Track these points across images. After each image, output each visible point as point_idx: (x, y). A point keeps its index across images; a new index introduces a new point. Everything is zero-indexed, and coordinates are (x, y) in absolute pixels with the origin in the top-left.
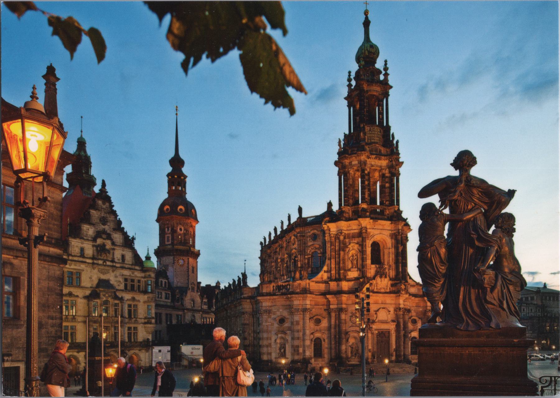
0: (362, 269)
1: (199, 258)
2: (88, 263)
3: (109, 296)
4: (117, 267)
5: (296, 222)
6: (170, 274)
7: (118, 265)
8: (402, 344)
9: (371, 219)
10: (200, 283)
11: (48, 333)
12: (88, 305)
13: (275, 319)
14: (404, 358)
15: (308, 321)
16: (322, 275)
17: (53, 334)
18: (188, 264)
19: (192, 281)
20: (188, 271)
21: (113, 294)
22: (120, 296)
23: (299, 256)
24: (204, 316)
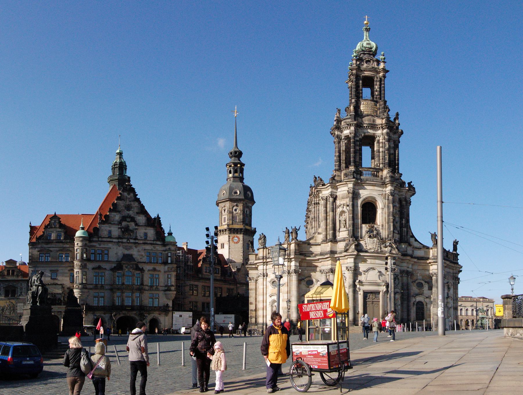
1: (255, 235)
3: (131, 268)
4: (139, 244)
7: (139, 242)
21: (135, 266)
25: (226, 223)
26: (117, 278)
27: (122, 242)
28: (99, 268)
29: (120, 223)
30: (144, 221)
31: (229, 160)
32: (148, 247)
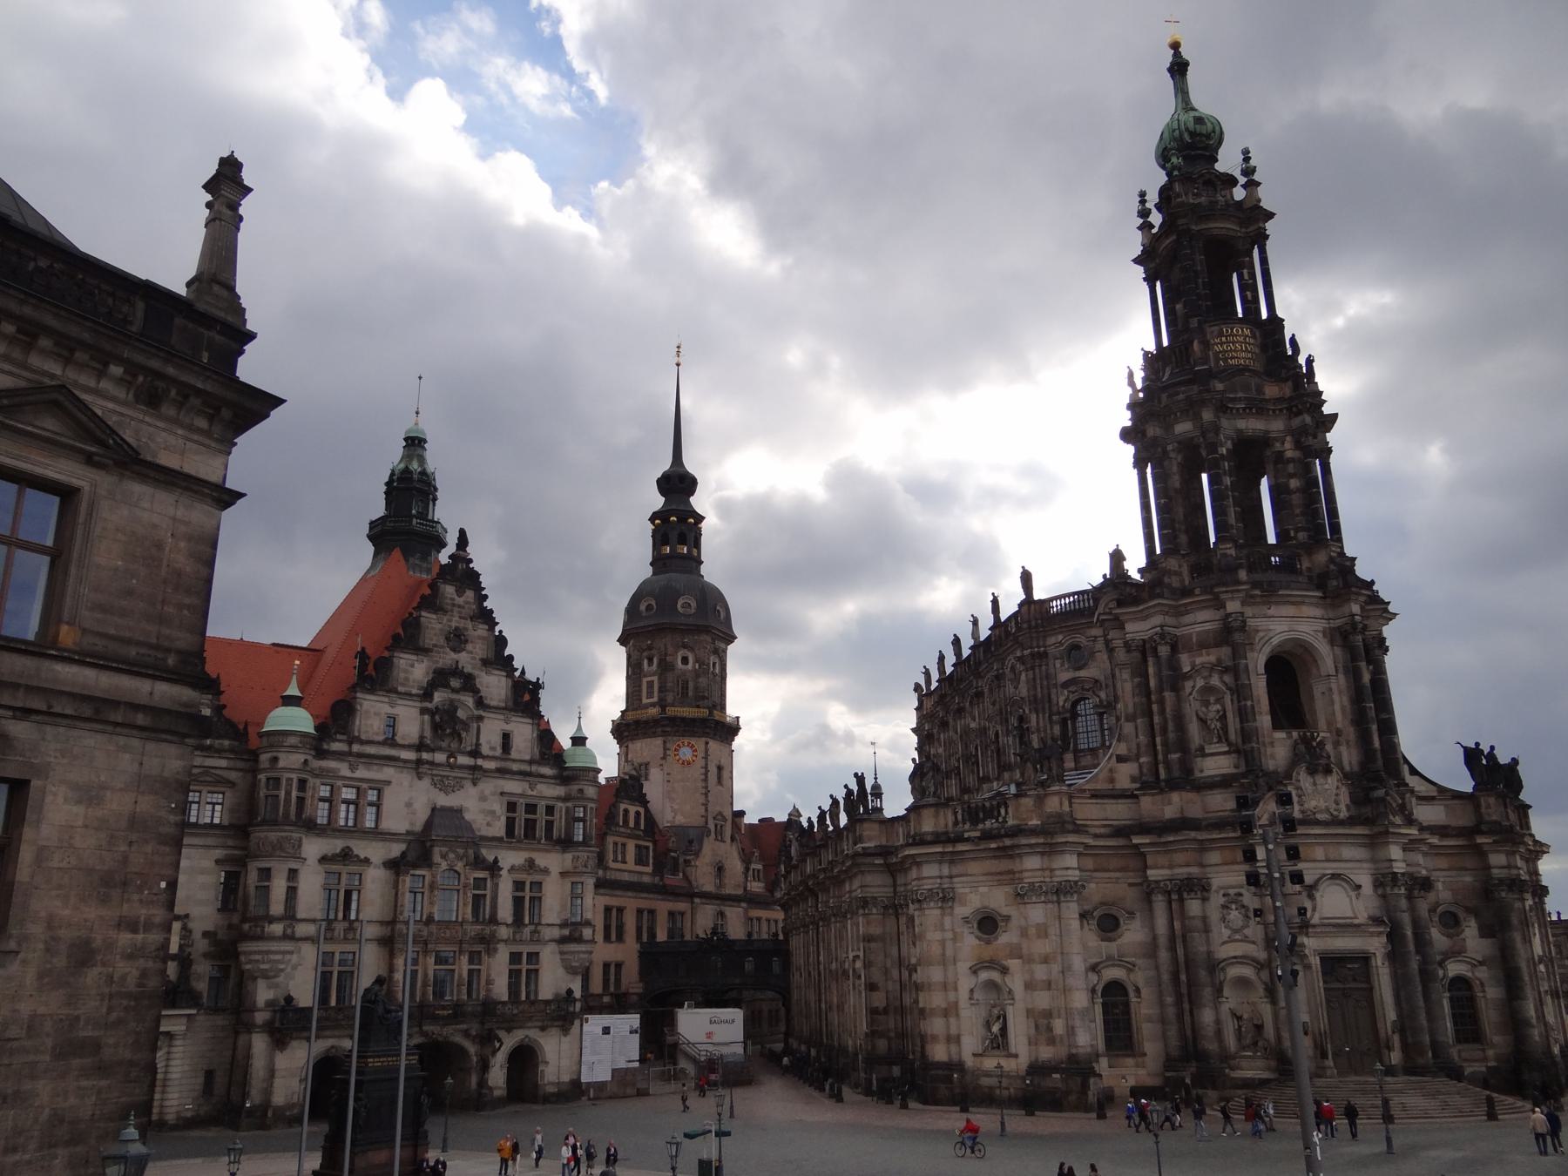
0: (1246, 749)
4: (486, 771)
5: (1015, 615)
6: (653, 789)
8: (1421, 1003)
10: (742, 813)
11: (110, 978)
12: (396, 886)
13: (966, 920)
14: (1435, 1056)
15: (1075, 924)
16: (1111, 770)
17: (131, 985)
18: (706, 758)
19: (718, 808)
20: (706, 780)
21: (471, 852)
22: (491, 858)
23: (1033, 717)
24: (755, 913)
25: (655, 699)
26: (408, 897)
27: (432, 763)
28: (346, 856)
29: (427, 695)
30: (503, 692)
31: (658, 502)
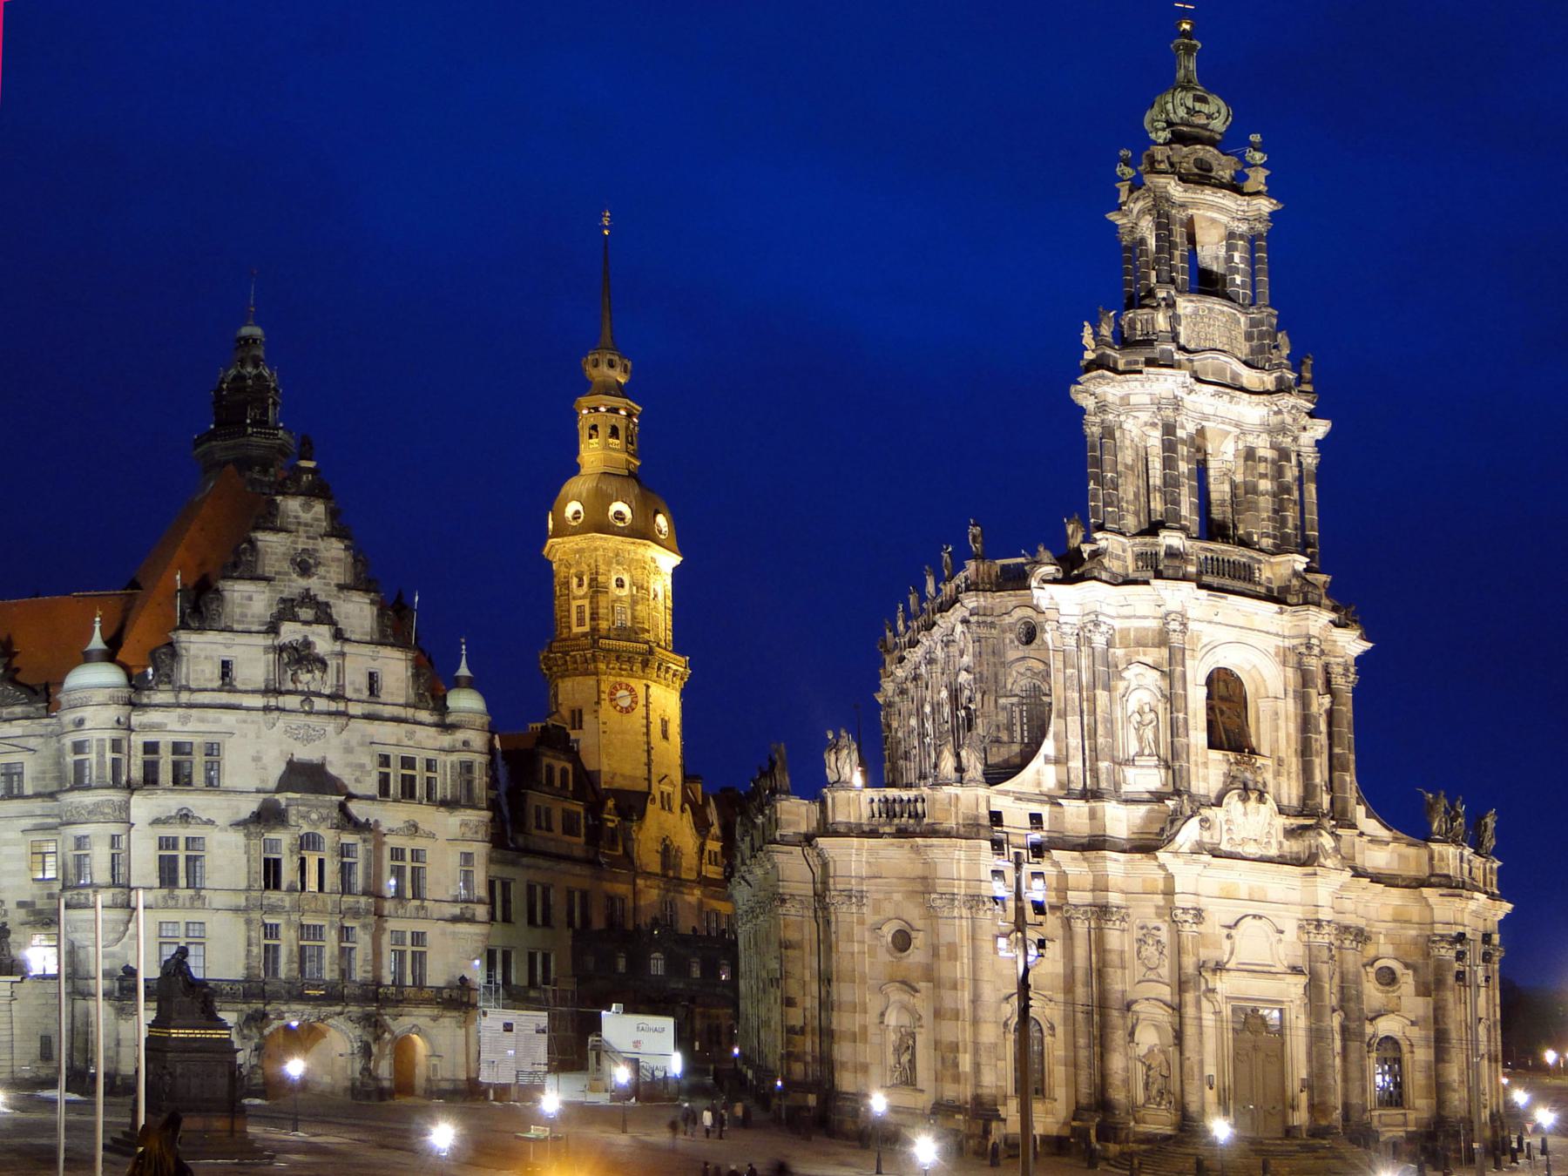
2: (248, 709)
9: (1201, 586)
19: (664, 771)
28: (185, 817)
32: (386, 732)
